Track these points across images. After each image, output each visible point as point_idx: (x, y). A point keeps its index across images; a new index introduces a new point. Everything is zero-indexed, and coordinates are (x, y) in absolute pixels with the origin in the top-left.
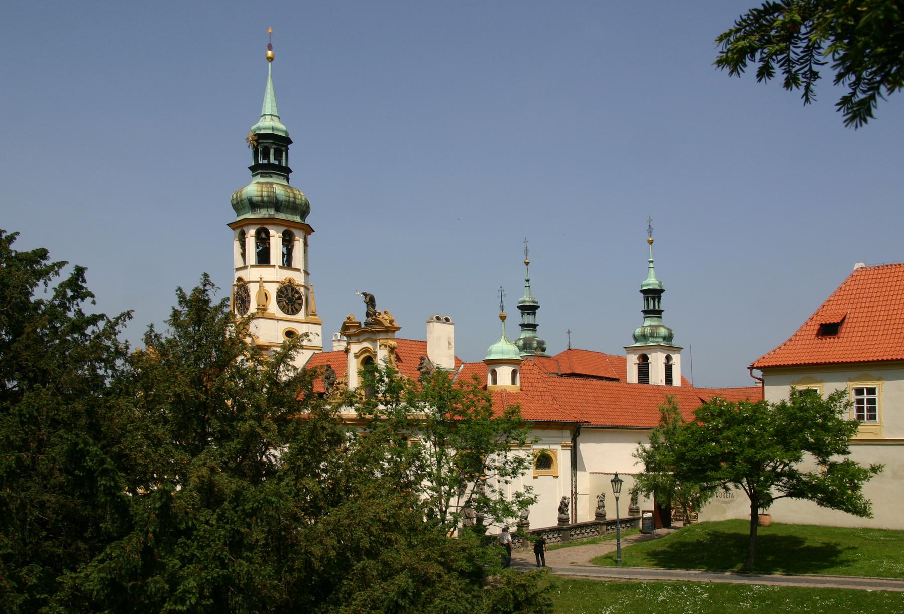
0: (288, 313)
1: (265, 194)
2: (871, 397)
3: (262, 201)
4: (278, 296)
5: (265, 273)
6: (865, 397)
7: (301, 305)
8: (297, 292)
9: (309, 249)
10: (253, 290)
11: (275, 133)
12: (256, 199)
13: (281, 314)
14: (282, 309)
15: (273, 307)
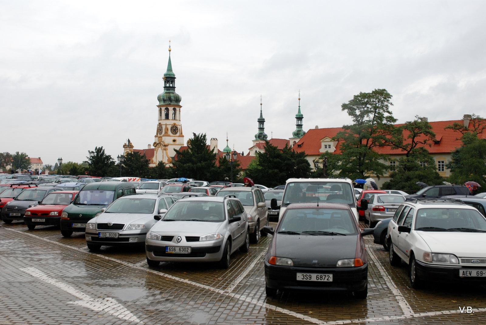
0: (174, 134)
1: (168, 97)
2: (440, 164)
3: (167, 99)
4: (171, 129)
5: (167, 122)
6: (441, 164)
7: (178, 131)
8: (177, 127)
9: (181, 112)
10: (164, 127)
11: (171, 76)
12: (166, 98)
13: (171, 134)
14: (172, 133)
15: (170, 132)
